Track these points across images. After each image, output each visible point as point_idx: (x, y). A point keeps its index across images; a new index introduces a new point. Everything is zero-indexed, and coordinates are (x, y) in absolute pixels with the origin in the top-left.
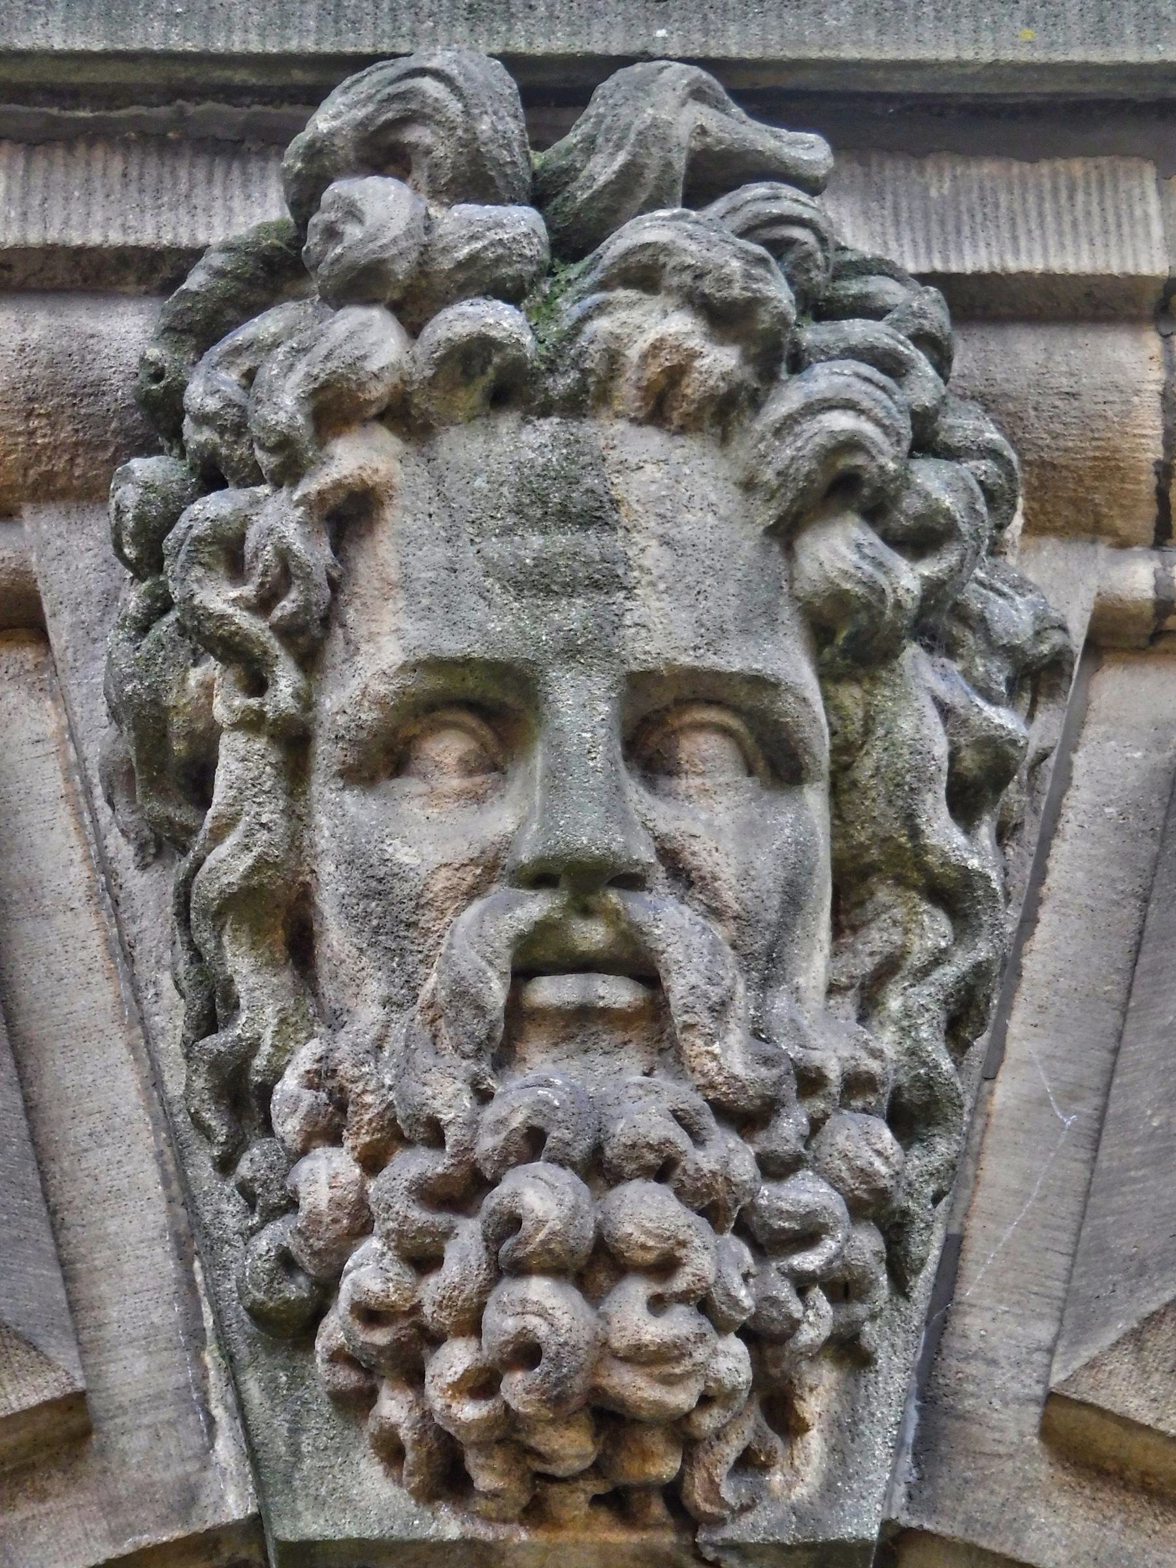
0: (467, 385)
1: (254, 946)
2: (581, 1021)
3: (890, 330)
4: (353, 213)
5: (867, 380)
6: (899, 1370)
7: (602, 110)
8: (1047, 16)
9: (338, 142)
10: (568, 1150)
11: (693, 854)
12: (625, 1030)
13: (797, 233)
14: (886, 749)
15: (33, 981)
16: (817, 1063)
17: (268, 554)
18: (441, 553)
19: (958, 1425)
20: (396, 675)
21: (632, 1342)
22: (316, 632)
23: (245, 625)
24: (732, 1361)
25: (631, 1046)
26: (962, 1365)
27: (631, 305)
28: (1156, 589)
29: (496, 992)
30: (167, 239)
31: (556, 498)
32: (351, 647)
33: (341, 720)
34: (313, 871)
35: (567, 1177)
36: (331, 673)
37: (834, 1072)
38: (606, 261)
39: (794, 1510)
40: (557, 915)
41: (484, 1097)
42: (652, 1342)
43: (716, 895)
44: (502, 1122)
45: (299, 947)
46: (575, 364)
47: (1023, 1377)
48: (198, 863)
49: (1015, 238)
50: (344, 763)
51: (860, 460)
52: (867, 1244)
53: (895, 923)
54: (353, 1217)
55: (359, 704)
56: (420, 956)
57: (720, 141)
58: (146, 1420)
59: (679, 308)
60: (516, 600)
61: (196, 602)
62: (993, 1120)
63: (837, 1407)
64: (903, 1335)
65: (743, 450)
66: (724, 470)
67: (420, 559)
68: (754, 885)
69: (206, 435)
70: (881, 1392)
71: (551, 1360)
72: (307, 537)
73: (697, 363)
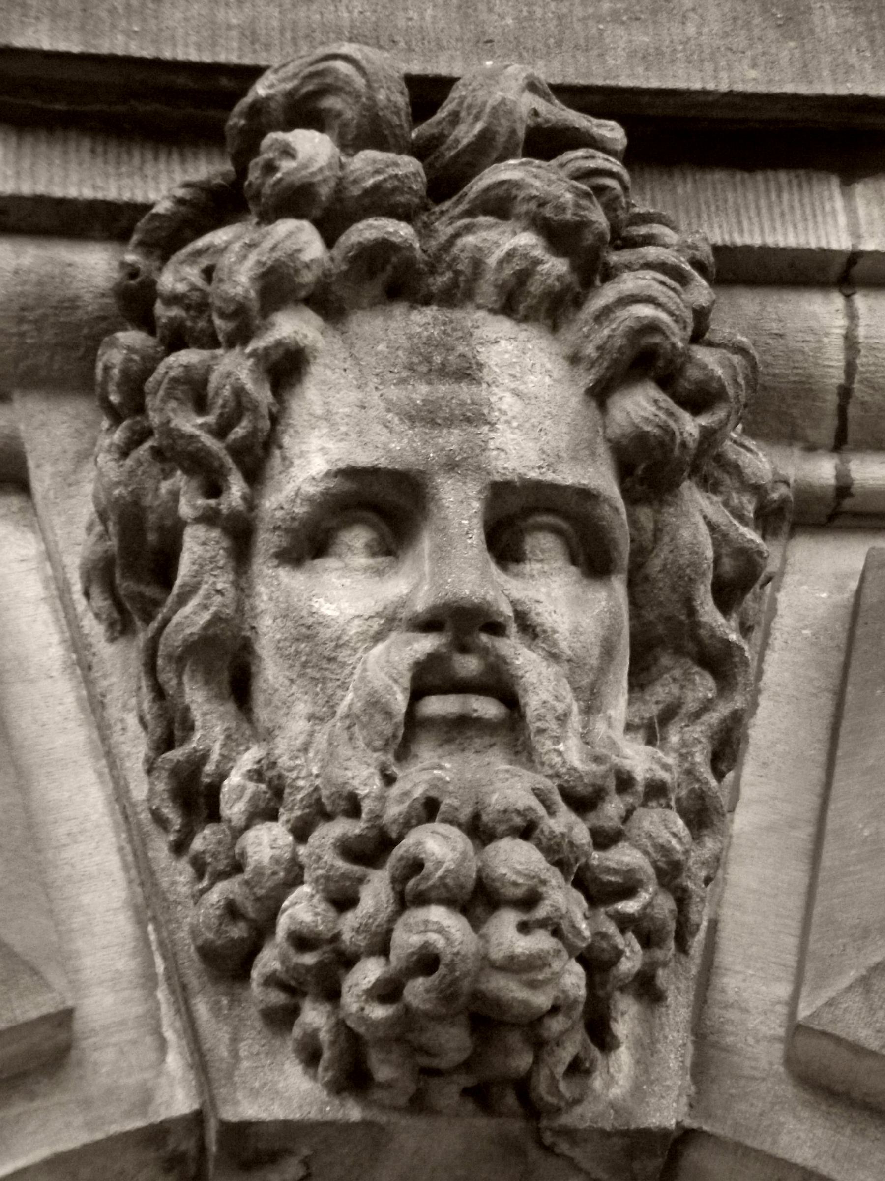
0: (371, 279)
1: (207, 683)
2: (459, 728)
3: (675, 254)
4: (288, 152)
5: (662, 283)
6: (683, 1007)
7: (463, 93)
8: (766, 63)
9: (273, 105)
11: (538, 614)
12: (491, 735)
14: (671, 551)
15: (24, 724)
16: (628, 768)
17: (227, 392)
18: (354, 396)
19: (723, 1055)
20: (322, 480)
21: (508, 954)
22: (260, 452)
24: (574, 979)
25: (495, 748)
26: (723, 1012)
27: (489, 227)
28: (837, 477)
29: (400, 702)
30: (126, 196)
31: (437, 359)
32: (287, 462)
33: (279, 514)
34: (253, 628)
35: (455, 833)
36: (270, 483)
37: (640, 775)
38: (472, 195)
39: (612, 1105)
40: (444, 650)
41: (389, 780)
42: (523, 954)
43: (555, 644)
44: (406, 794)
45: (239, 687)
46: (450, 267)
47: (768, 1022)
48: (166, 621)
49: (740, 223)
50: (279, 547)
51: (657, 339)
52: (666, 905)
53: (674, 680)
54: (288, 871)
55: (293, 501)
56: (338, 683)
57: (547, 121)
58: (113, 1040)
59: (525, 229)
60: (410, 428)
61: (172, 425)
62: (734, 840)
63: (638, 1030)
64: (684, 981)
65: (570, 335)
66: (555, 348)
67: (338, 400)
68: (582, 638)
69: (175, 312)
70: (672, 1021)
71: (447, 965)
72: (256, 381)
73: (539, 268)
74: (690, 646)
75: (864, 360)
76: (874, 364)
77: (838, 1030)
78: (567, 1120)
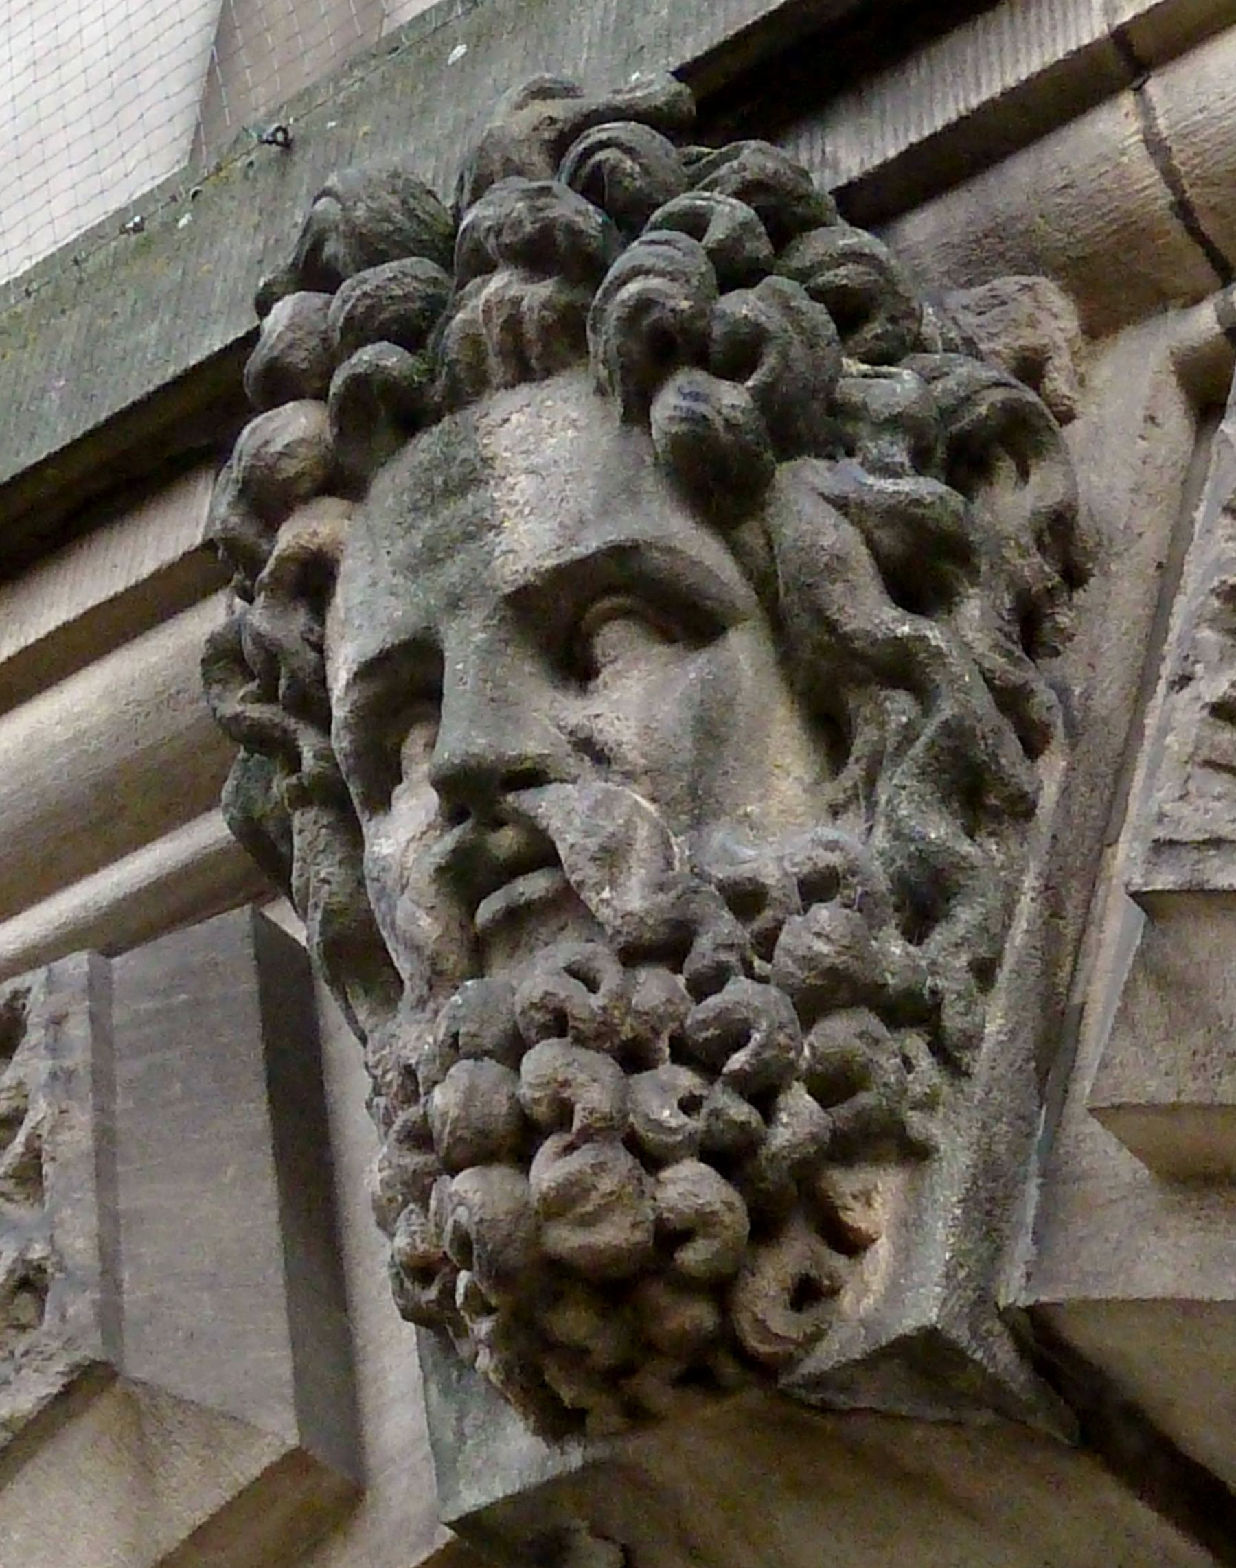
10: (478, 1041)
11: (601, 731)
13: (600, 156)
20: (346, 694)
23: (256, 715)
31: (439, 481)
39: (862, 1322)
42: (549, 1187)
43: (624, 760)
51: (655, 314)
74: (859, 668)
75: (1182, 156)
76: (1196, 154)
77: (1126, 1096)
78: (810, 1366)
